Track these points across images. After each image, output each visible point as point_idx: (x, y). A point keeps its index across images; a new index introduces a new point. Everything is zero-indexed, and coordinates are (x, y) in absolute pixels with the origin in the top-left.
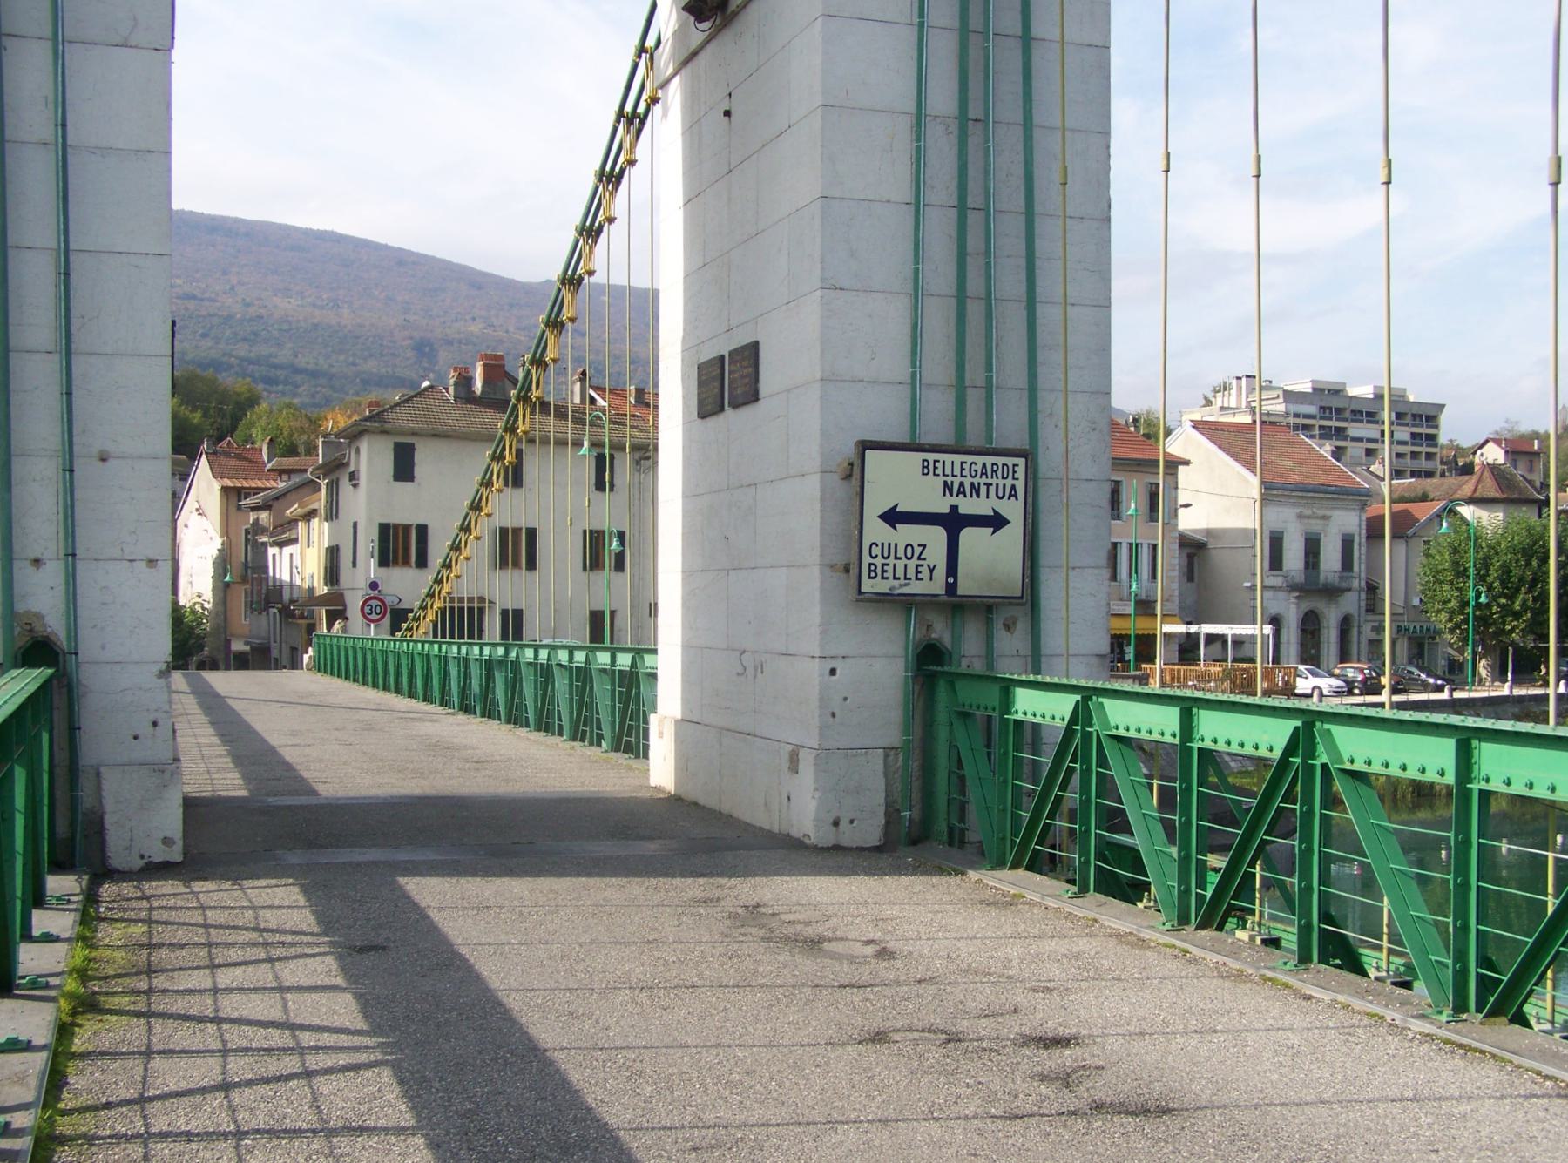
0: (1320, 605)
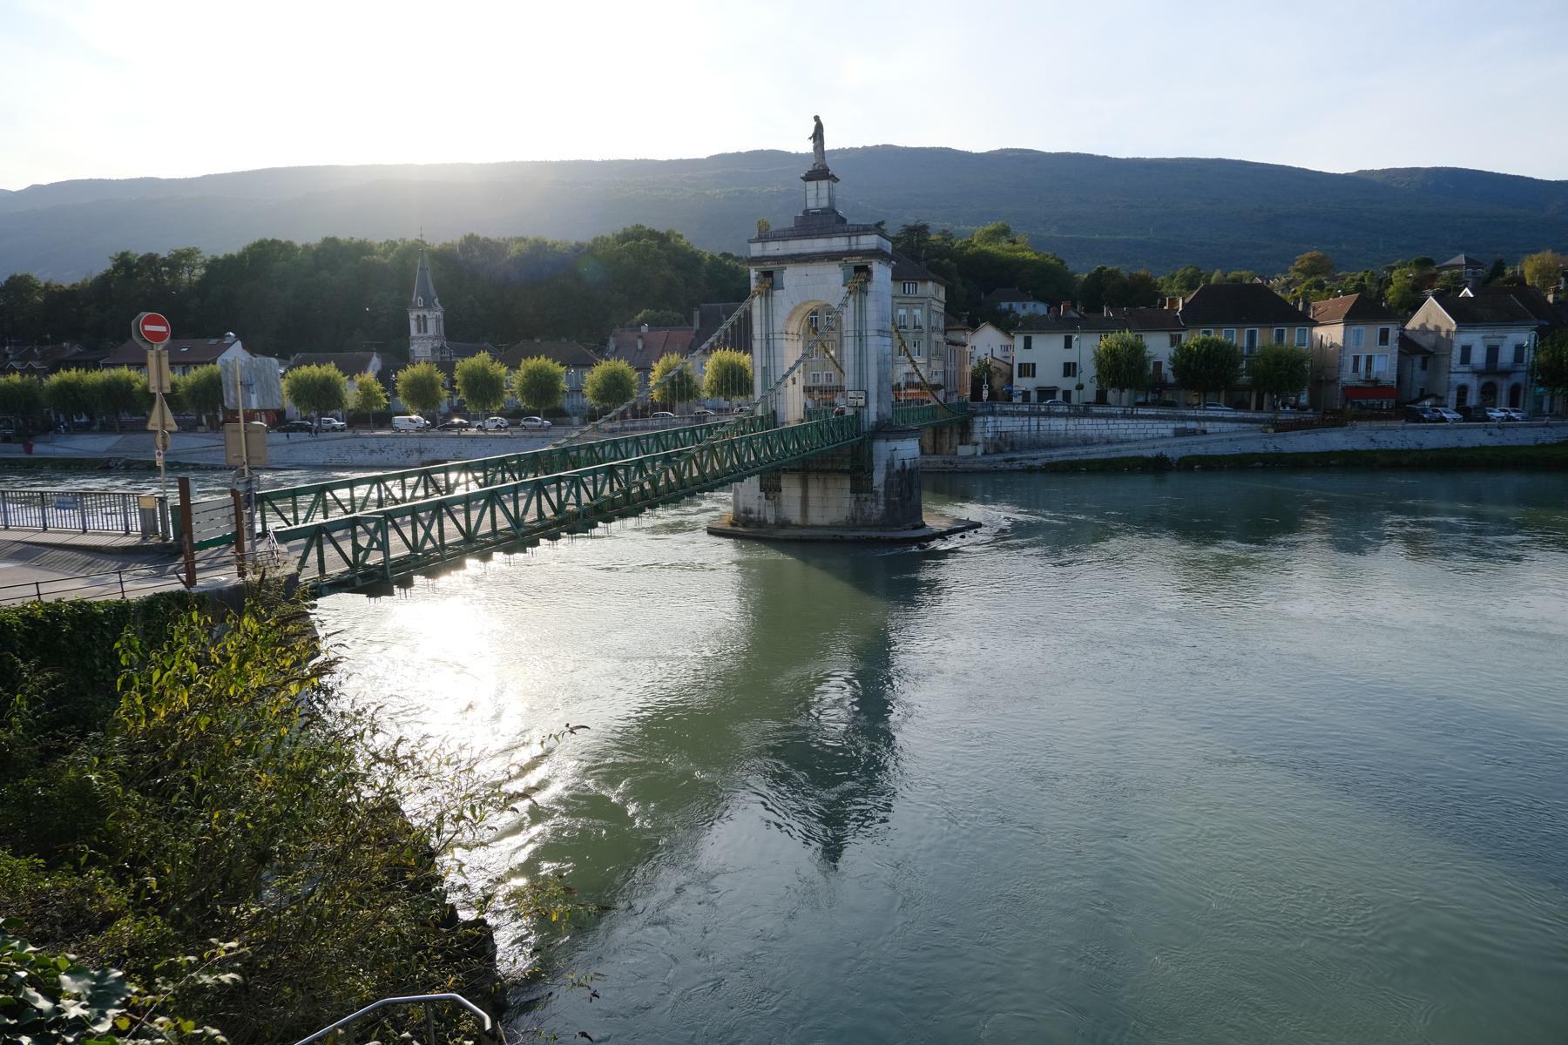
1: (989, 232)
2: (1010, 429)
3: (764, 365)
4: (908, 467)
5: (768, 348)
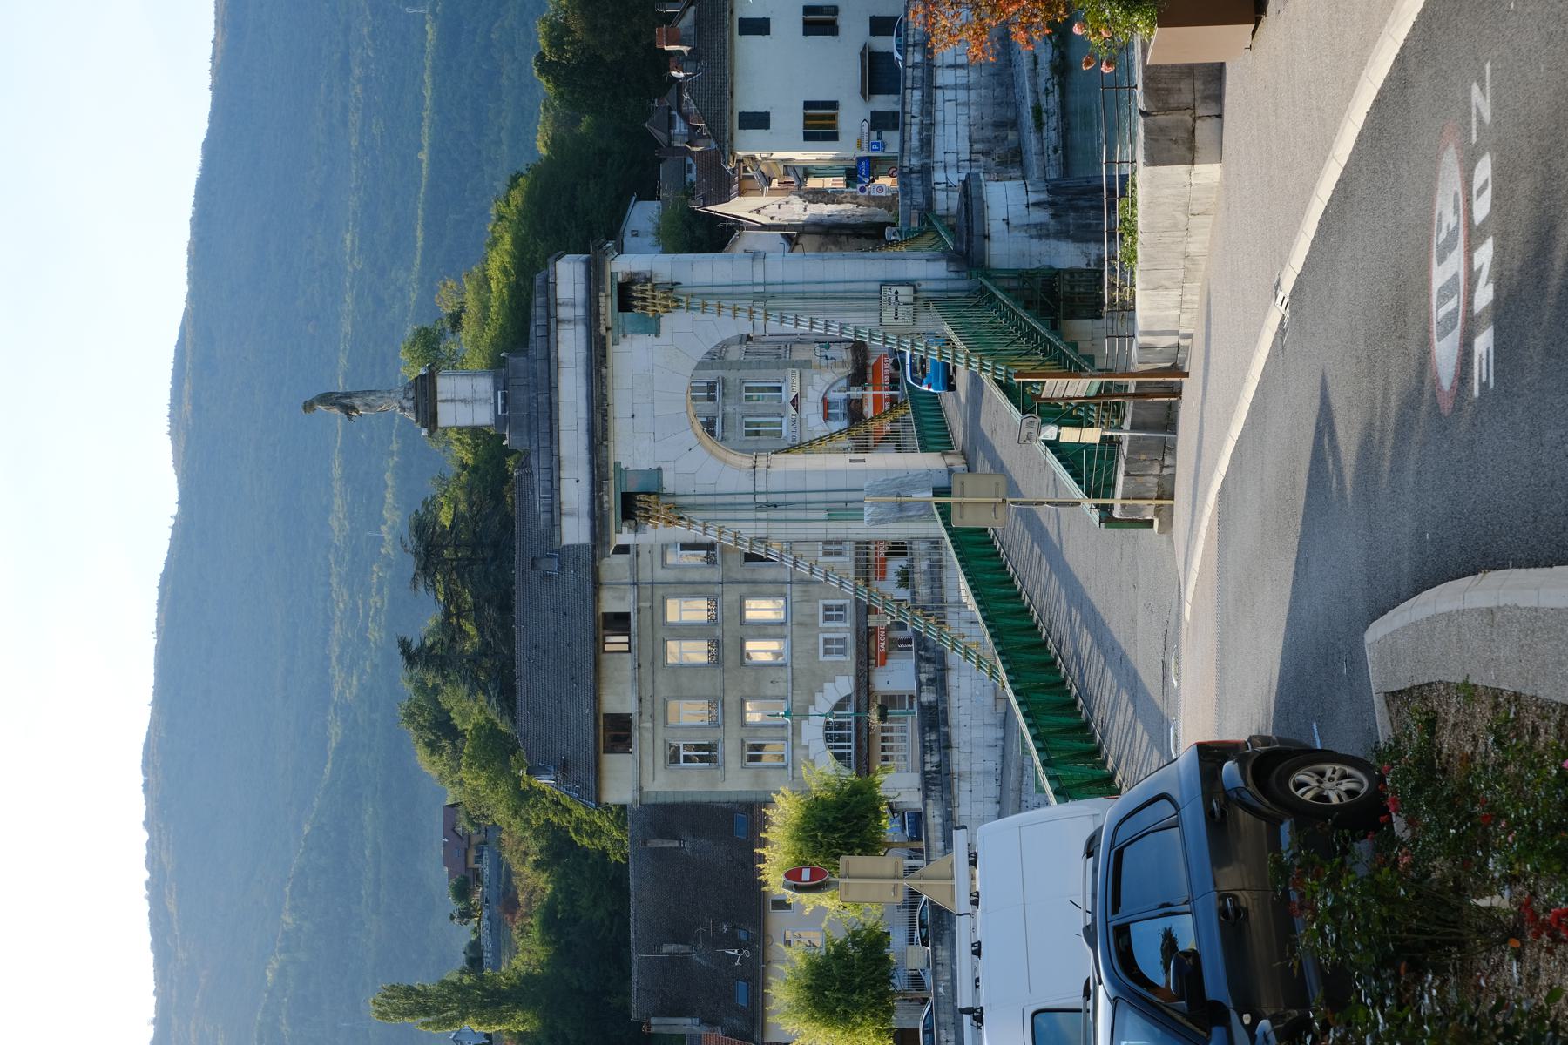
2: (964, 131)
3: (823, 515)
4: (1044, 196)
5: (787, 505)
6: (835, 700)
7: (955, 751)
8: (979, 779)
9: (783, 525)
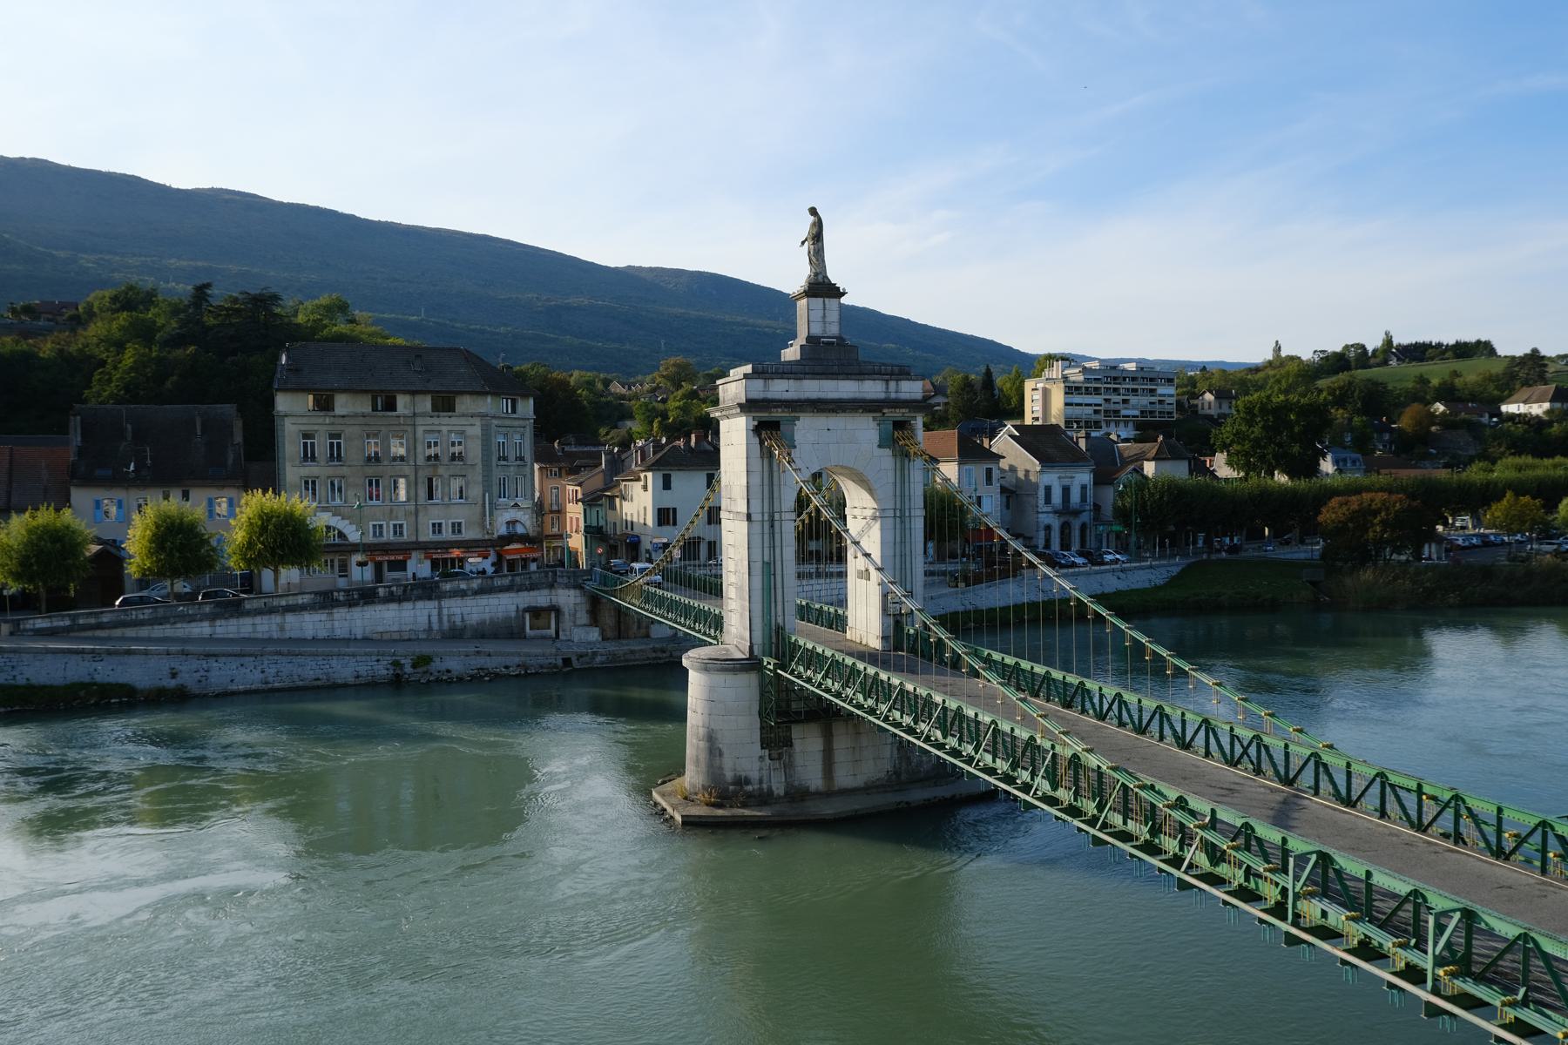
0: (1071, 519)
1: (318, 307)
5: (772, 534)
6: (345, 531)
7: (346, 610)
8: (329, 625)
9: (760, 531)
